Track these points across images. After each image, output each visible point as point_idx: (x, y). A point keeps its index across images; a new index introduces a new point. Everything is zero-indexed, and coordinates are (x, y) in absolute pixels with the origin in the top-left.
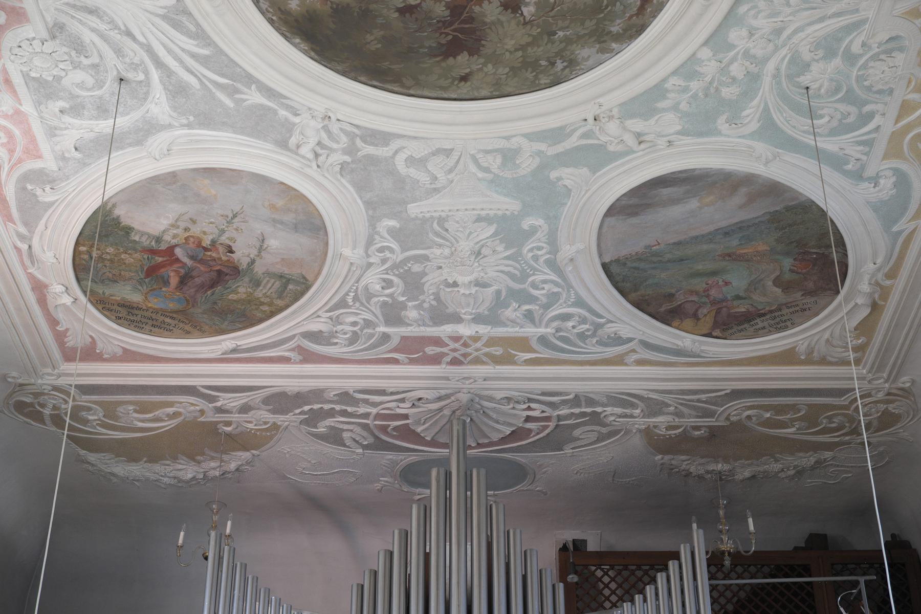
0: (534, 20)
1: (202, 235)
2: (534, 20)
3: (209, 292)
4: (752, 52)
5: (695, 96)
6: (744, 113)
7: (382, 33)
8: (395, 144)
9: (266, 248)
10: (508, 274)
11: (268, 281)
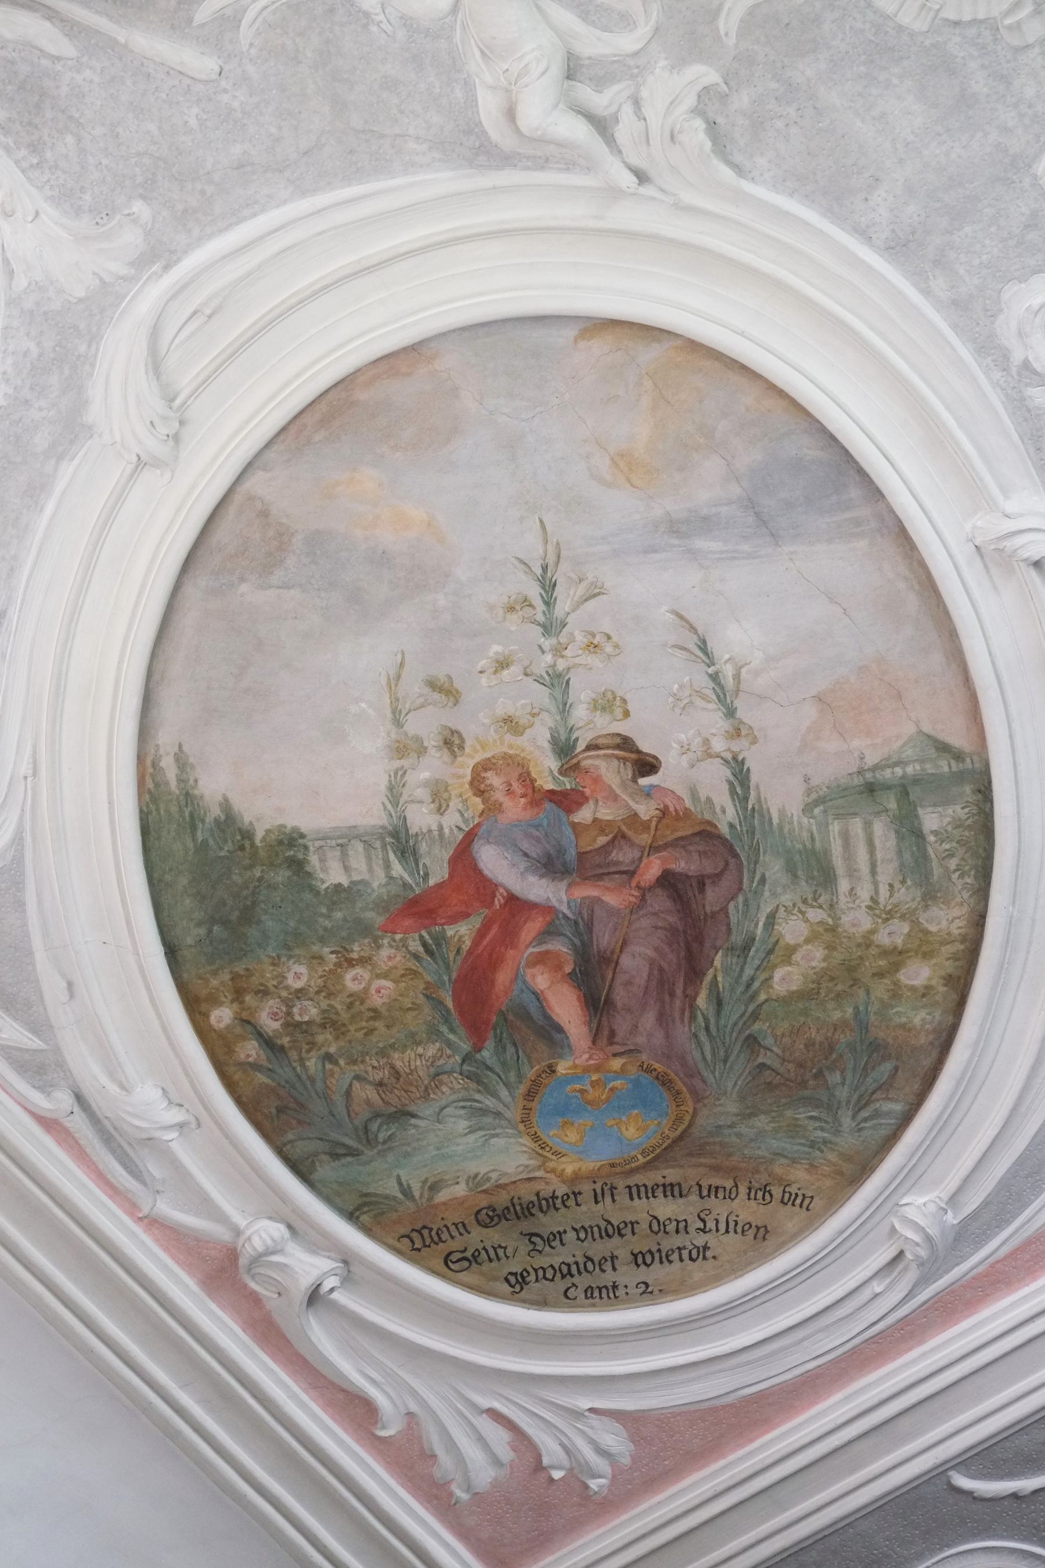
1: (509, 738)
3: (701, 1001)
9: (737, 677)
11: (845, 836)
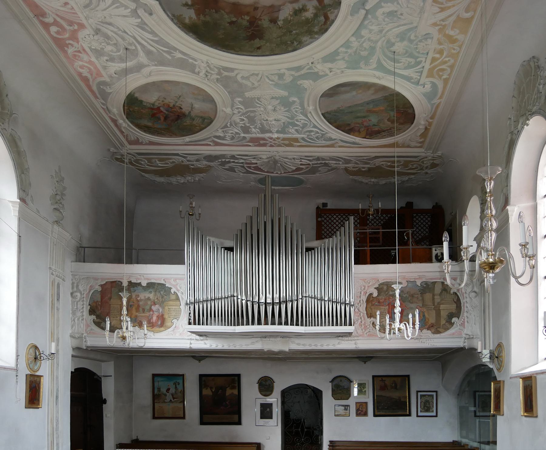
4: (371, 38)
5: (350, 55)
6: (371, 61)
8: (236, 72)
10: (287, 117)
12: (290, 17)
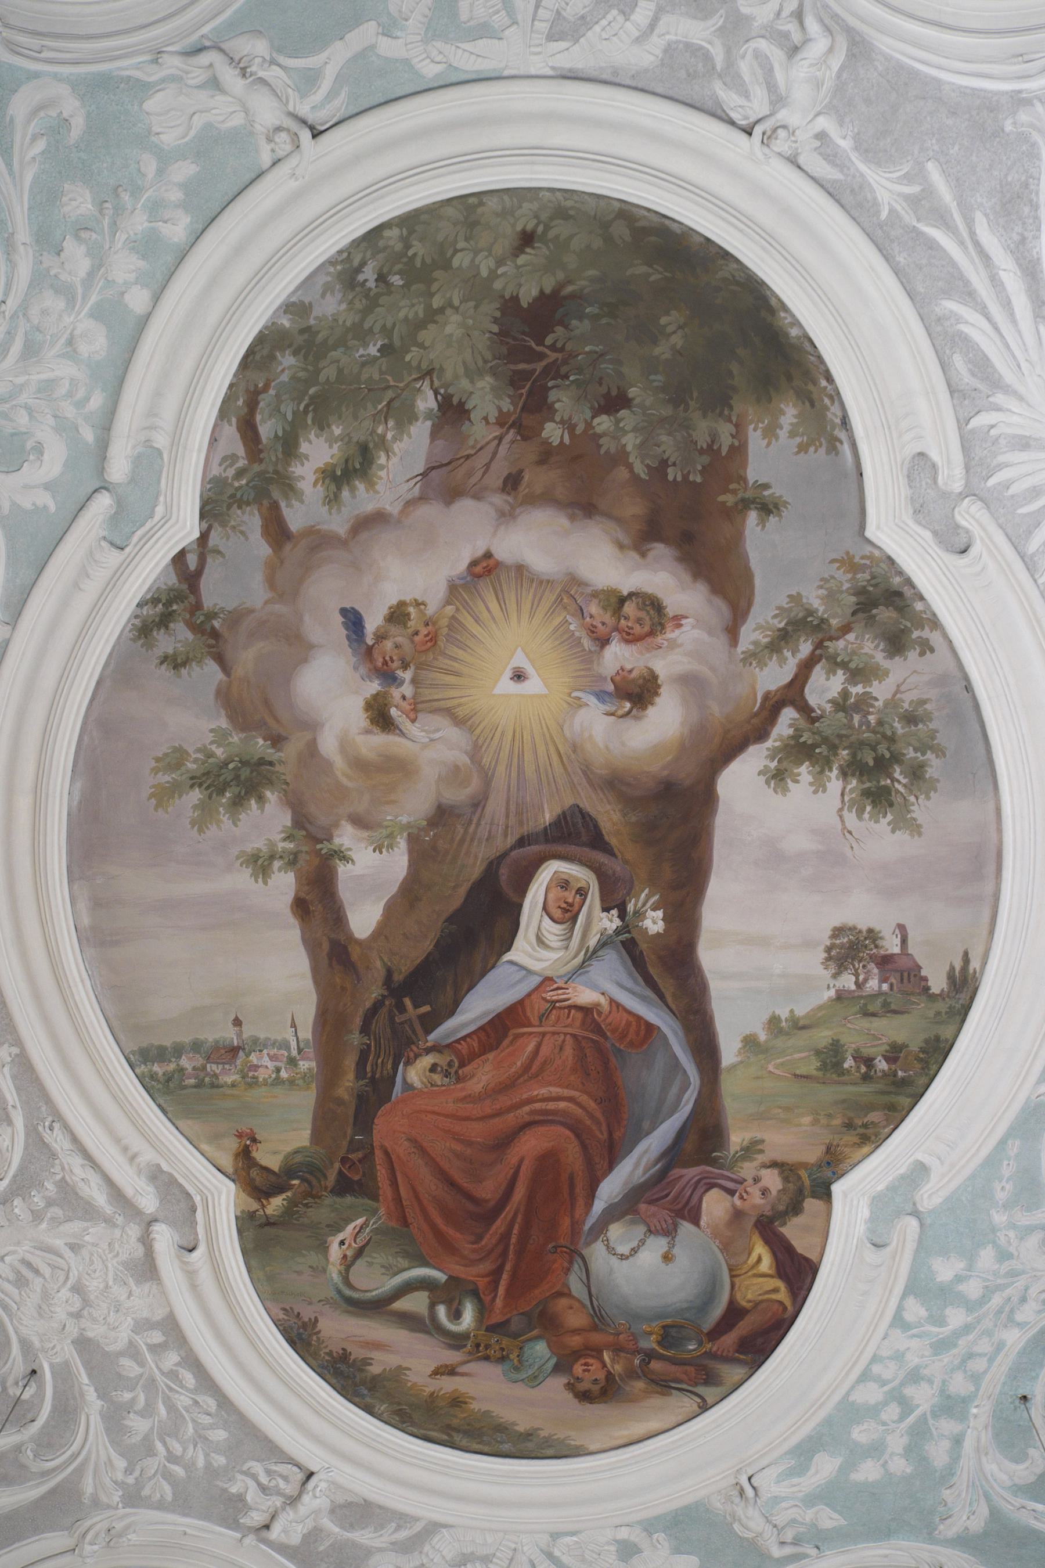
0: (415, 380)
2: (415, 380)
7: (657, 351)
12: (389, 436)
